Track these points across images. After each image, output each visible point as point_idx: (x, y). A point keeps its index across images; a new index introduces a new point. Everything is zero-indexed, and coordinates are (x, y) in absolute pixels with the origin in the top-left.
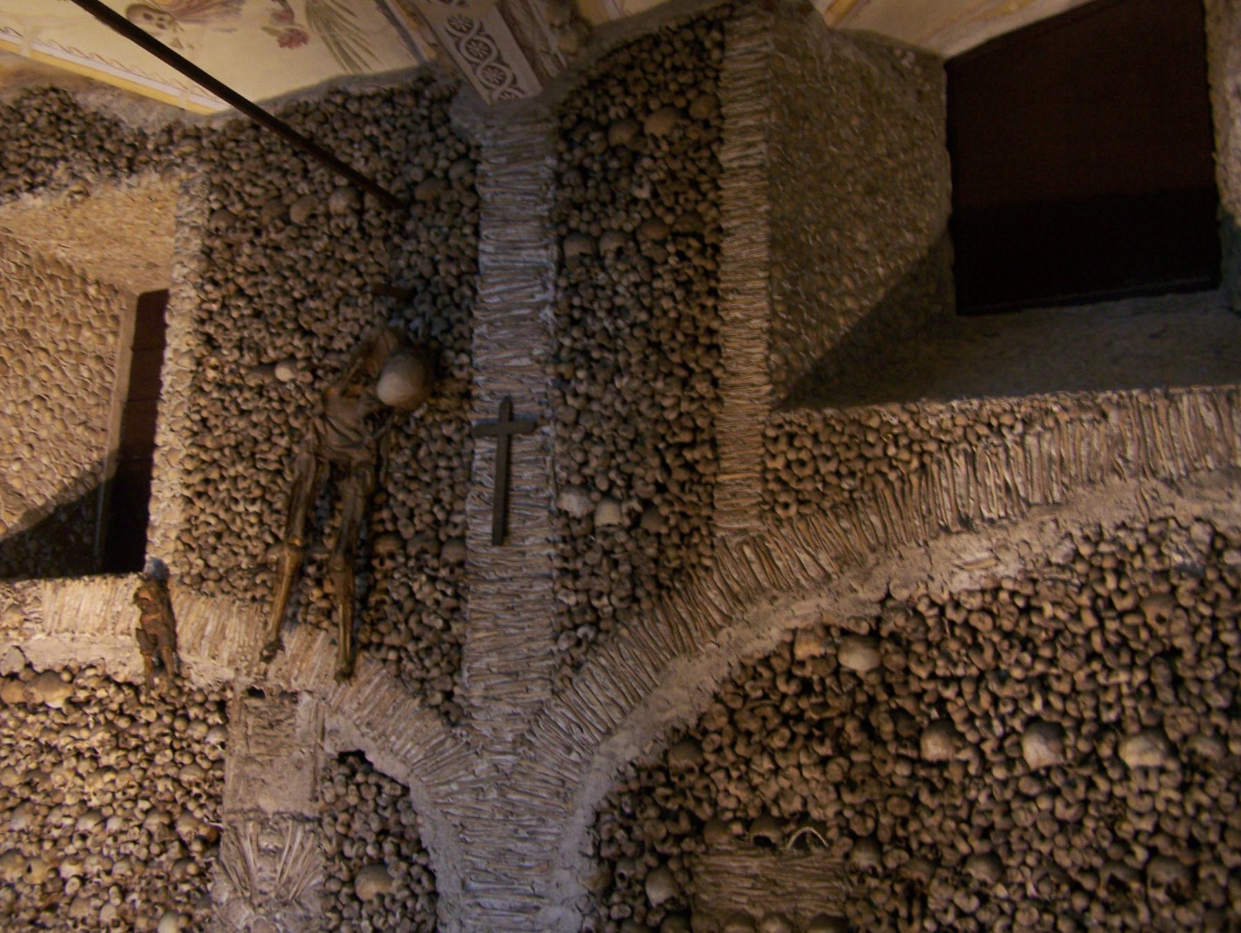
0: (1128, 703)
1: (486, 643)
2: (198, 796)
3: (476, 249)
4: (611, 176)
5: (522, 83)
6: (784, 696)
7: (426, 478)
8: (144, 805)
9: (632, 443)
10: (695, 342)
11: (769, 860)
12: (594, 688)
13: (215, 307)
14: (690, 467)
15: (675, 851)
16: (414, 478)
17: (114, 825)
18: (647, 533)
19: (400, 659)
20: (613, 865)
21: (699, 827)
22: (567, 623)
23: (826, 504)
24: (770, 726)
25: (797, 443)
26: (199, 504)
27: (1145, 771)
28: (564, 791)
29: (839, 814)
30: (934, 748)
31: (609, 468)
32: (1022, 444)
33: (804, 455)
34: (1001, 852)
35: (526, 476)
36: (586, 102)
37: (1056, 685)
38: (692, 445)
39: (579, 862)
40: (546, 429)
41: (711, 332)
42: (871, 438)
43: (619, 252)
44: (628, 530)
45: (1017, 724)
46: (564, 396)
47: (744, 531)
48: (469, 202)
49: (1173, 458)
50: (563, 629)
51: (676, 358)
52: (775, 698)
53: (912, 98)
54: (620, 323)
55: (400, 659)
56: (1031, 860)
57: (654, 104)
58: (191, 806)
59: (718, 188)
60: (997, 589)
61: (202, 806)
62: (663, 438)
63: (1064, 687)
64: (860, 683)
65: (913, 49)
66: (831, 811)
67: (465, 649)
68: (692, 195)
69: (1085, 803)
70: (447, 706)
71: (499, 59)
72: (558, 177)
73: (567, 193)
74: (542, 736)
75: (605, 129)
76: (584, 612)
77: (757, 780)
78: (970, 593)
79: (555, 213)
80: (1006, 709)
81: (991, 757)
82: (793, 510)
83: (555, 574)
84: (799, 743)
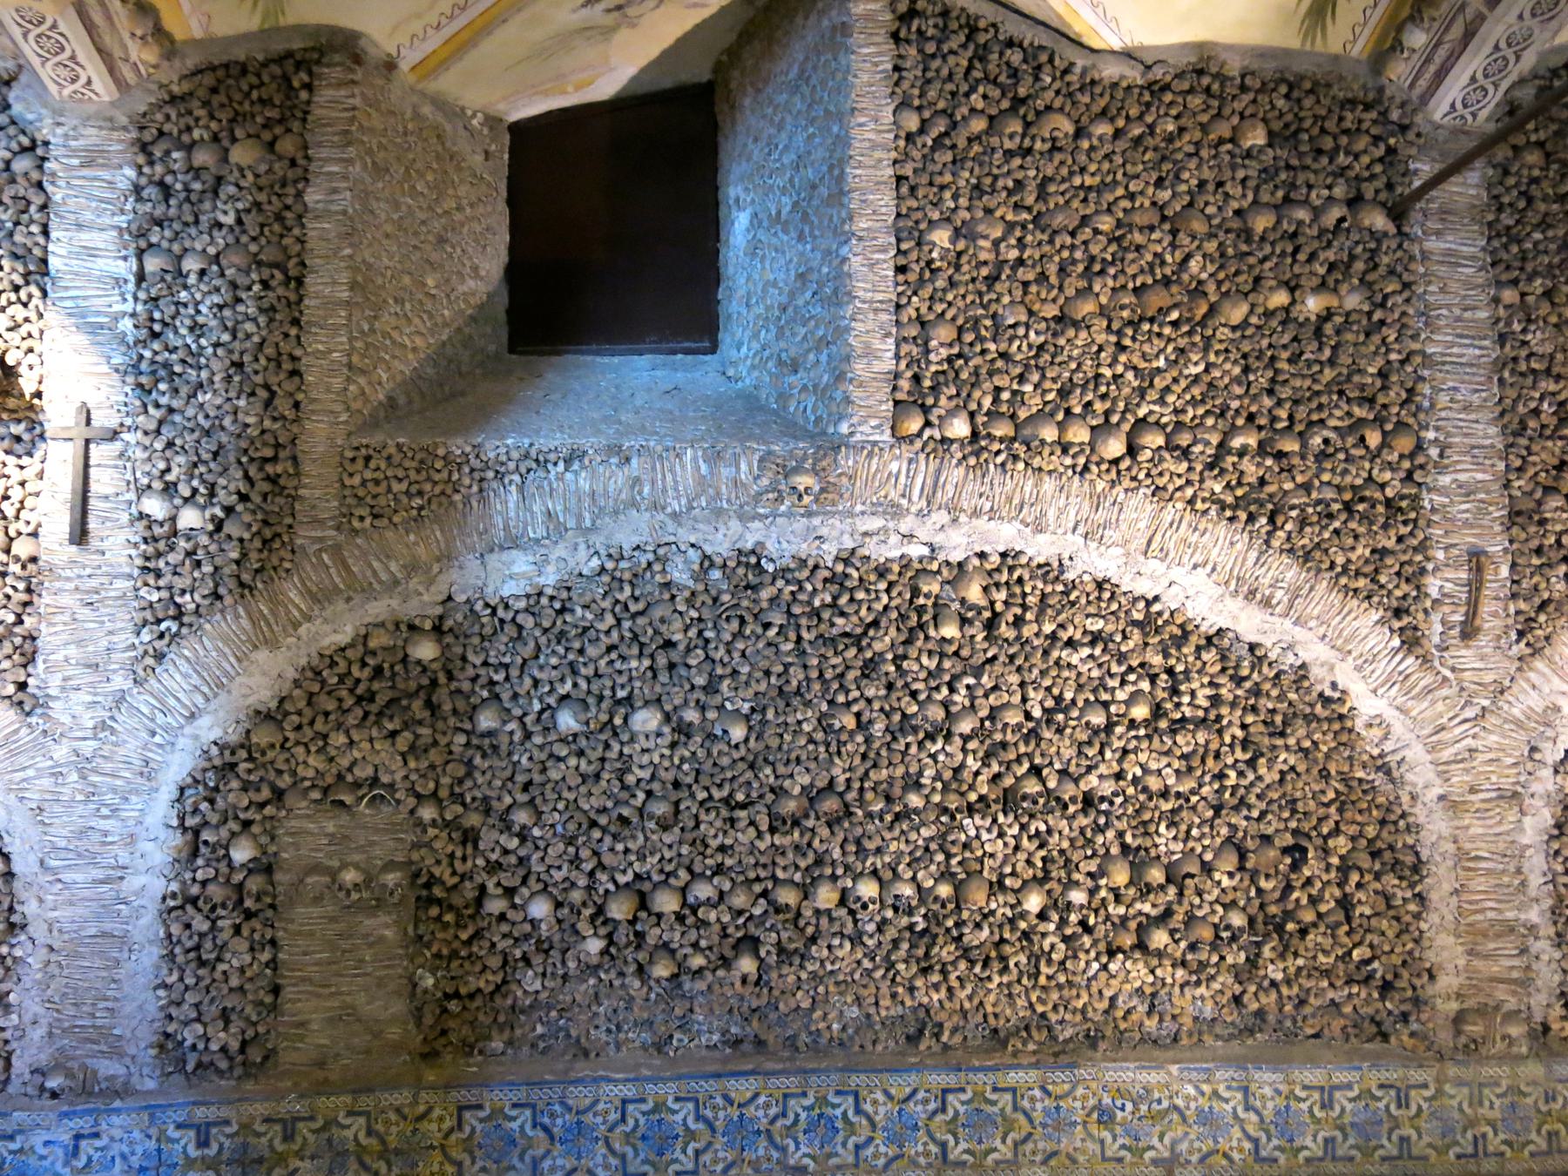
0: (637, 684)
1: (65, 637)
4: (194, 197)
5: (97, 85)
6: (358, 681)
9: (216, 454)
11: (345, 818)
12: (178, 677)
14: (273, 480)
15: (258, 817)
18: (229, 537)
20: (197, 832)
21: (279, 795)
22: (150, 618)
23: (396, 519)
24: (346, 706)
25: (372, 464)
28: (148, 771)
30: (486, 721)
31: (192, 477)
34: (538, 801)
35: (104, 481)
36: (168, 117)
37: (583, 671)
38: (274, 459)
39: (163, 834)
40: (125, 436)
41: (294, 359)
42: (438, 465)
43: (202, 273)
44: (211, 534)
45: (552, 701)
46: (145, 406)
47: (321, 539)
48: (38, 200)
49: (678, 498)
50: (145, 623)
51: (259, 379)
52: (349, 683)
53: (479, 158)
54: (203, 342)
56: (561, 806)
57: (239, 133)
59: (303, 226)
60: (540, 594)
64: (425, 670)
66: (398, 776)
67: (39, 643)
68: (277, 228)
69: (603, 760)
70: (20, 696)
71: (73, 58)
72: (137, 190)
73: (148, 207)
74: (125, 720)
75: (189, 148)
77: (333, 753)
78: (518, 597)
79: (134, 227)
81: (530, 728)
82: (368, 521)
83: (136, 572)
84: (372, 718)
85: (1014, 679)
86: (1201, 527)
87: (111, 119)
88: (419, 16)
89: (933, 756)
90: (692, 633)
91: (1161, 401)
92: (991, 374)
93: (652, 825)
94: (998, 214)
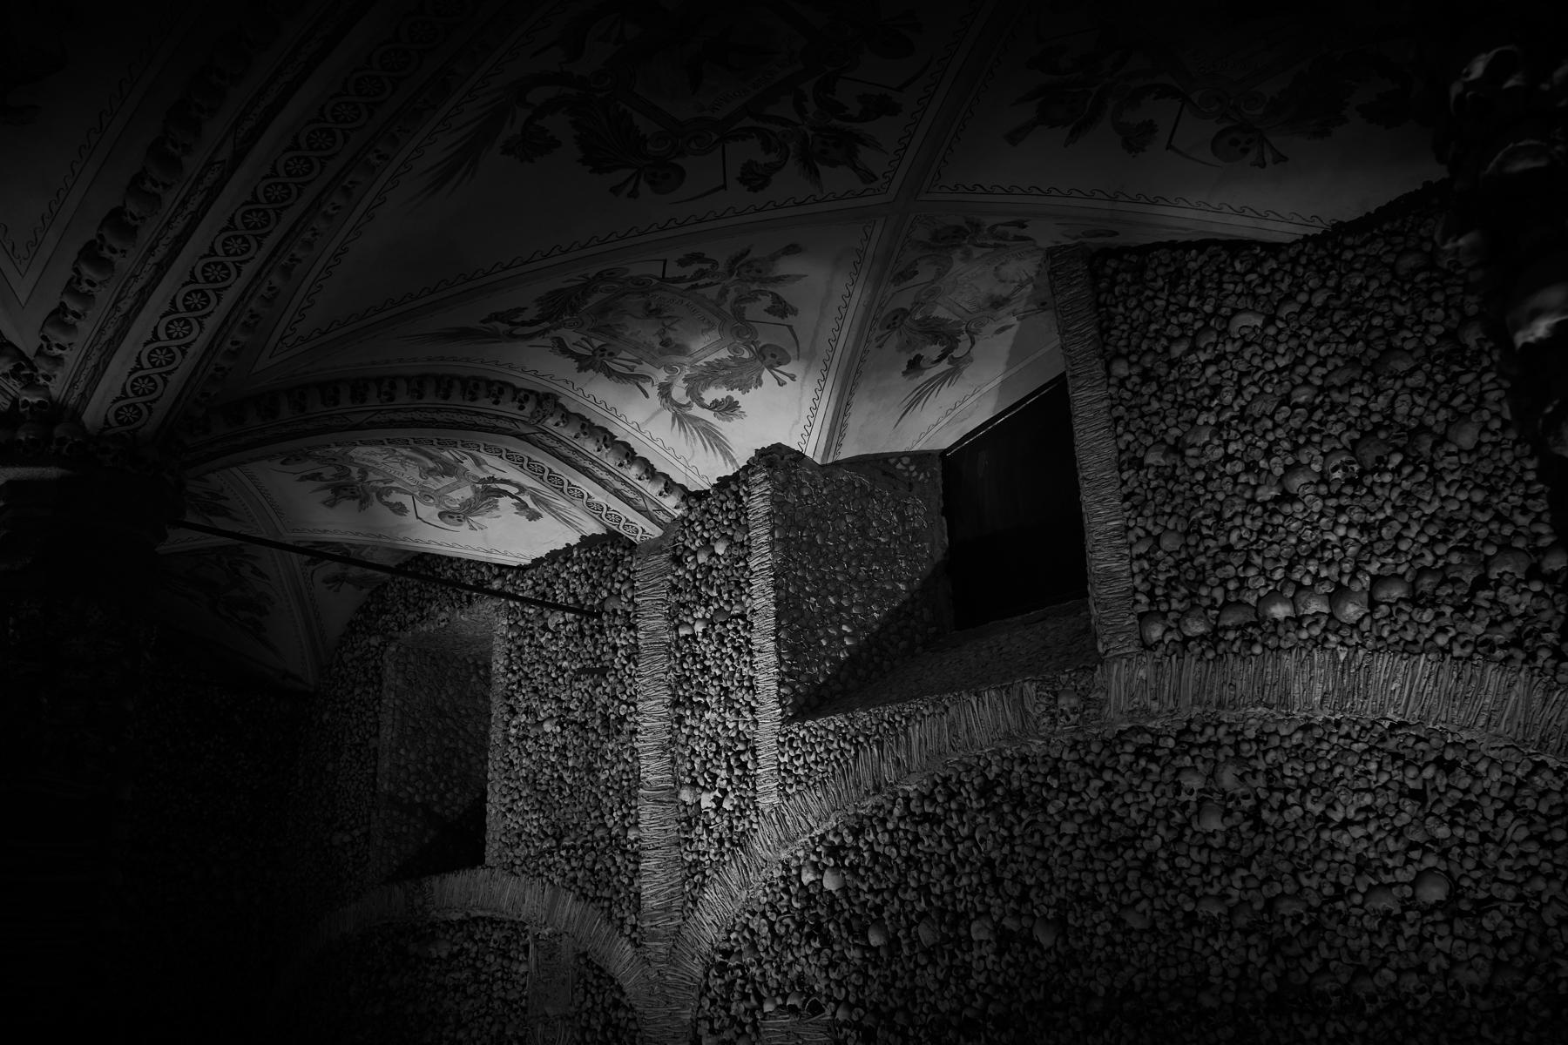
2: (516, 1010)
3: (636, 638)
5: (647, 530)
7: (616, 787)
8: (489, 1019)
10: (742, 687)
13: (515, 687)
16: (612, 788)
17: (475, 1034)
19: (611, 906)
23: (811, 783)
26: (509, 816)
27: (981, 942)
29: (827, 986)
32: (906, 733)
33: (798, 752)
42: (831, 738)
43: (705, 633)
44: (715, 811)
45: (913, 917)
55: (611, 906)
58: (512, 1016)
61: (518, 1016)
62: (730, 749)
63: (937, 890)
65: (905, 454)
75: (695, 553)
76: (696, 866)
80: (908, 908)
85: (1285, 867)
86: (1466, 676)
87: (660, 547)
88: (797, 422)
89: (1217, 954)
90: (1006, 849)
91: (1395, 551)
92: (1215, 567)
93: (990, 1025)
94: (1200, 421)
